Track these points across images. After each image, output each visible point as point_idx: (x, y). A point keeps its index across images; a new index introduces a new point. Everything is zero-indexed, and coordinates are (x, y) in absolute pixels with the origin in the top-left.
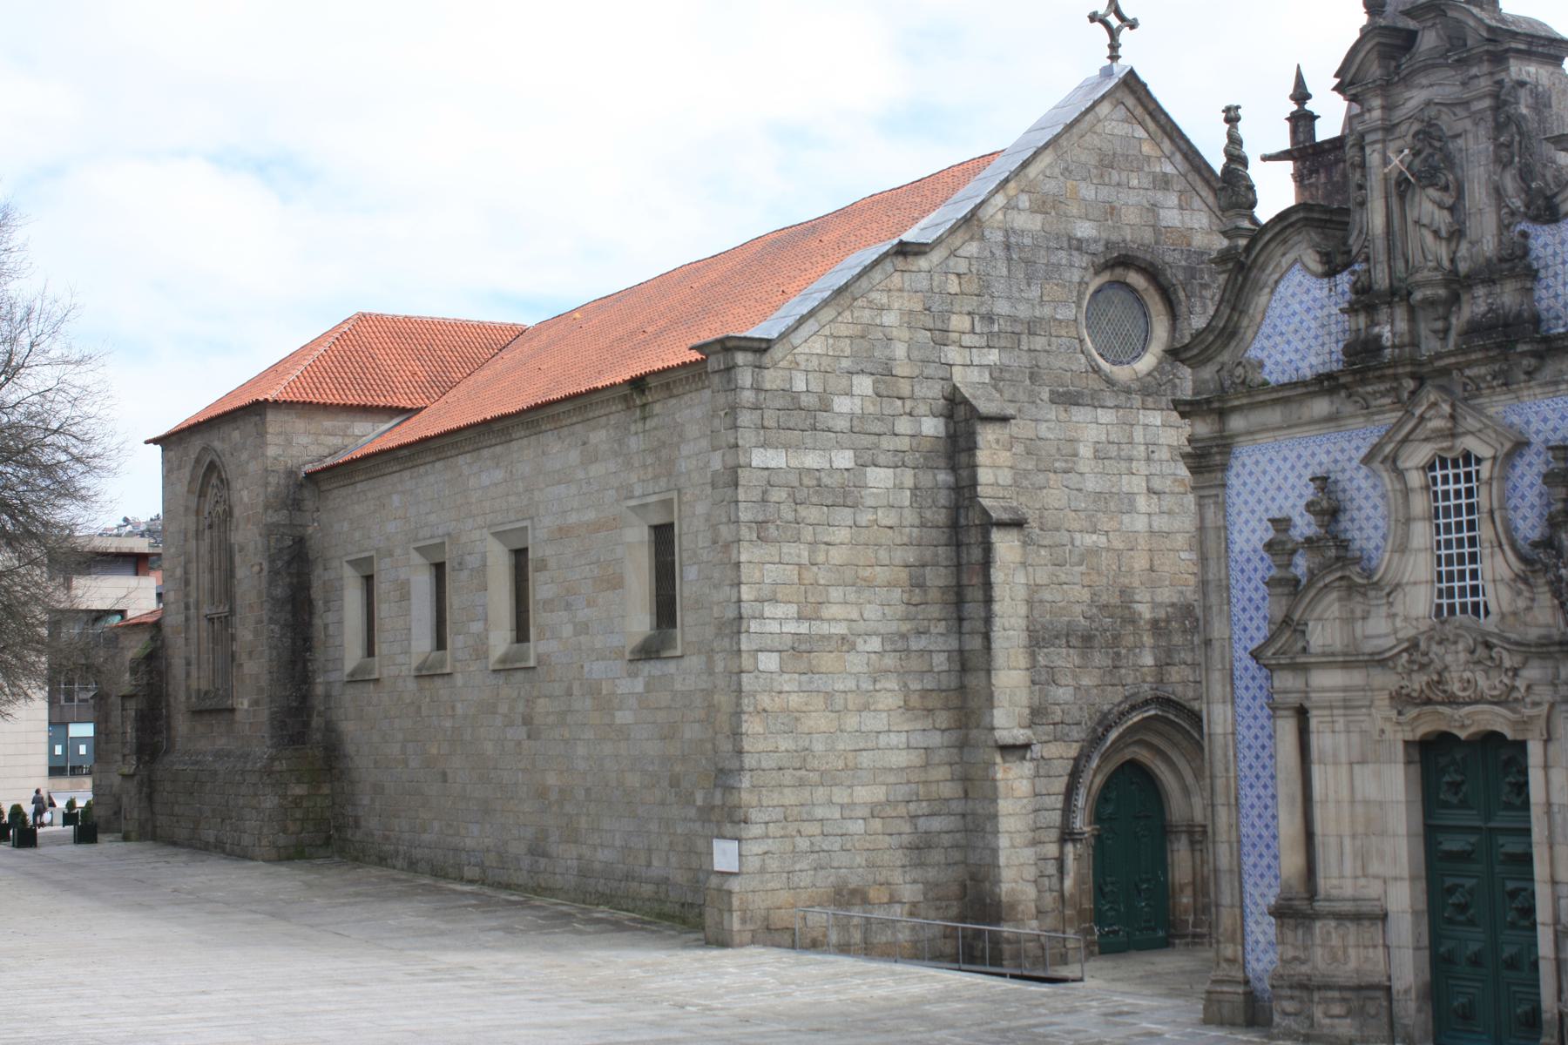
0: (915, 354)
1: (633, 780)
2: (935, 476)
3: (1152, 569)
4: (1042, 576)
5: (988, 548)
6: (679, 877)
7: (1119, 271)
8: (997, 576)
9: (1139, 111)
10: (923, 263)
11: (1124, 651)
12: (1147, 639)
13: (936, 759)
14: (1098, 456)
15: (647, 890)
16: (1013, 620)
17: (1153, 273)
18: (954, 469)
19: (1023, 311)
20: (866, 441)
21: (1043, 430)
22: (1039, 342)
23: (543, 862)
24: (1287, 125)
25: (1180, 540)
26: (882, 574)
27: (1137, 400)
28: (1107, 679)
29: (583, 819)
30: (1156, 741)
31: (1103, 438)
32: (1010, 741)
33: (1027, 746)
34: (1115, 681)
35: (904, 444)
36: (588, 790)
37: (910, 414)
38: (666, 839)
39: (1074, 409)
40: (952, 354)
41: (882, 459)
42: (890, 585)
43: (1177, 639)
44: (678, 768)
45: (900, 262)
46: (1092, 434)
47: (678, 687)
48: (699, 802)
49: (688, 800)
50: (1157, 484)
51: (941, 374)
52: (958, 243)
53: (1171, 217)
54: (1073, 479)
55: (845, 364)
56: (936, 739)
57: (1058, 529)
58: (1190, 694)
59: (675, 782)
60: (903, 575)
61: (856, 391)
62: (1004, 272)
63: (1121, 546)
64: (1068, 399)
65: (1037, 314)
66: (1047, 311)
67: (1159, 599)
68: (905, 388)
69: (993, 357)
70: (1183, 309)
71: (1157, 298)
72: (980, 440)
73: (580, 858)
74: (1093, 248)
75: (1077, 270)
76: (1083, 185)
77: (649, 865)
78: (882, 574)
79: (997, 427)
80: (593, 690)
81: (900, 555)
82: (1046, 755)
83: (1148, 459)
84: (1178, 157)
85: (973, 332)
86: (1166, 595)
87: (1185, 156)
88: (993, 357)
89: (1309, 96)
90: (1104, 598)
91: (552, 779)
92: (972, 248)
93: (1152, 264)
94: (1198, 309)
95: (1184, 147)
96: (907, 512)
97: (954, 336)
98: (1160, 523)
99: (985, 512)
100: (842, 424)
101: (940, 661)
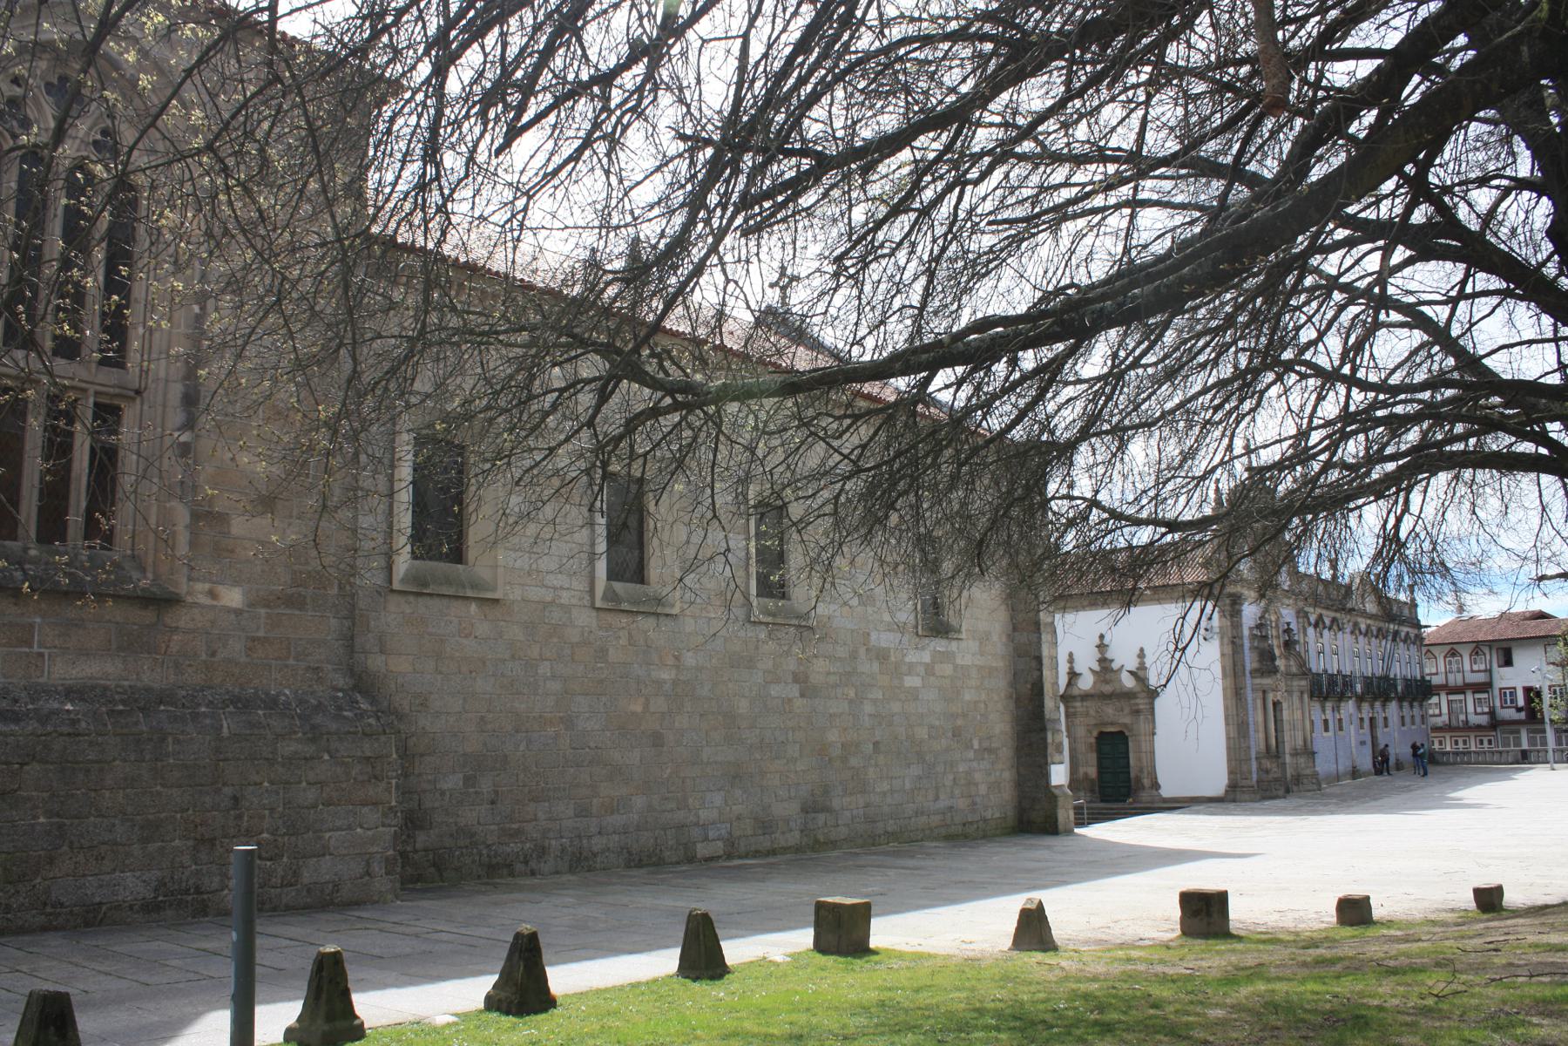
1: (922, 733)
6: (962, 804)
15: (936, 820)
23: (821, 818)
29: (871, 770)
36: (876, 744)
38: (951, 777)
44: (959, 722)
47: (959, 661)
48: (976, 746)
49: (969, 746)
59: (956, 733)
73: (867, 806)
77: (937, 798)
80: (882, 655)
91: (833, 736)
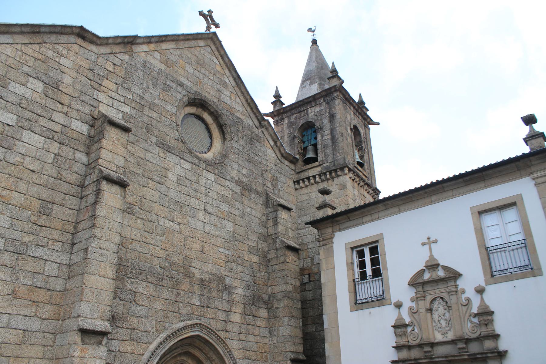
0: (78, 87)
2: (74, 153)
3: (203, 251)
4: (136, 234)
5: (98, 192)
7: (200, 110)
8: (101, 211)
9: (216, 53)
10: (93, 48)
11: (183, 293)
12: (197, 289)
13: (33, 341)
14: (179, 182)
16: (107, 244)
17: (216, 116)
18: (88, 154)
19: (148, 97)
20: (27, 115)
21: (149, 156)
22: (155, 115)
24: (272, 106)
25: (219, 242)
26: (17, 198)
27: (204, 165)
28: (170, 308)
30: (197, 353)
31: (183, 175)
32: (91, 327)
33: (103, 334)
34: (176, 310)
35: (58, 128)
37: (66, 114)
39: (169, 154)
40: (101, 96)
41: (37, 129)
42: (21, 207)
43: (214, 293)
45: (80, 41)
46: (178, 170)
50: (210, 209)
51: (93, 102)
52: (118, 51)
53: (227, 100)
54: (163, 189)
55: (25, 68)
56: (36, 324)
57: (150, 212)
58: (219, 327)
60: (36, 204)
61: (29, 85)
62: (141, 76)
63: (187, 234)
64: (167, 148)
65: (156, 102)
66: (160, 103)
67: (205, 269)
68: (66, 100)
69: (126, 109)
70: (228, 136)
71: (217, 130)
72: (107, 135)
74: (189, 90)
75: (180, 95)
76: (187, 65)
78: (17, 198)
79: (120, 132)
81: (35, 190)
82: (122, 349)
83: (206, 195)
84: (231, 79)
85: (116, 92)
86: (210, 268)
87: (235, 79)
88: (126, 109)
89: (280, 97)
90: (174, 259)
92: (126, 58)
93: (216, 111)
94: (235, 138)
95: (235, 75)
96: (47, 166)
97: (105, 89)
98: (209, 228)
99: (101, 171)
100: (11, 98)
101: (51, 269)
